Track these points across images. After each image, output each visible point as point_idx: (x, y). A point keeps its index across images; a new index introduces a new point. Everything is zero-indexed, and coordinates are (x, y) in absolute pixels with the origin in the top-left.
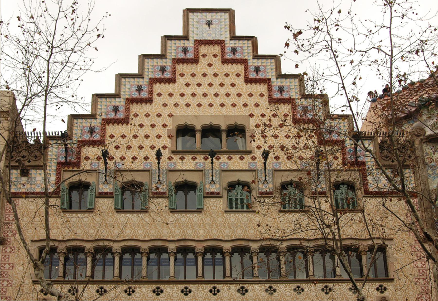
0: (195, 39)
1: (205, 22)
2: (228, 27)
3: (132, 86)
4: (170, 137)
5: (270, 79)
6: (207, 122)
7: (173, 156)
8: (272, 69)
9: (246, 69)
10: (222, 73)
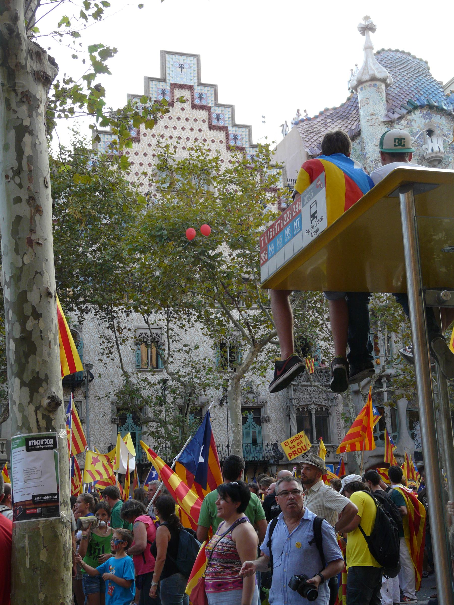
1: (178, 65)
2: (196, 72)
7: (156, 194)
8: (229, 118)
9: (210, 115)
10: (192, 118)
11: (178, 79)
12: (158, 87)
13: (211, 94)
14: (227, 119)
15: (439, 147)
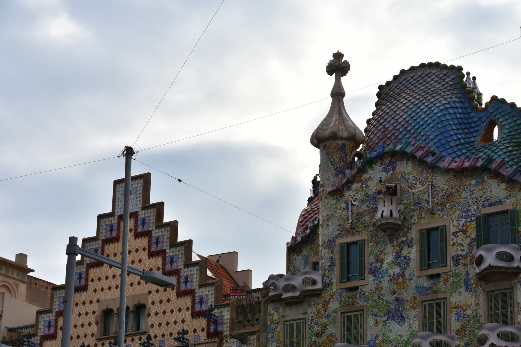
4: (97, 323)
5: (165, 250)
7: (97, 343)
12: (107, 223)
13: (154, 216)
15: (383, 211)
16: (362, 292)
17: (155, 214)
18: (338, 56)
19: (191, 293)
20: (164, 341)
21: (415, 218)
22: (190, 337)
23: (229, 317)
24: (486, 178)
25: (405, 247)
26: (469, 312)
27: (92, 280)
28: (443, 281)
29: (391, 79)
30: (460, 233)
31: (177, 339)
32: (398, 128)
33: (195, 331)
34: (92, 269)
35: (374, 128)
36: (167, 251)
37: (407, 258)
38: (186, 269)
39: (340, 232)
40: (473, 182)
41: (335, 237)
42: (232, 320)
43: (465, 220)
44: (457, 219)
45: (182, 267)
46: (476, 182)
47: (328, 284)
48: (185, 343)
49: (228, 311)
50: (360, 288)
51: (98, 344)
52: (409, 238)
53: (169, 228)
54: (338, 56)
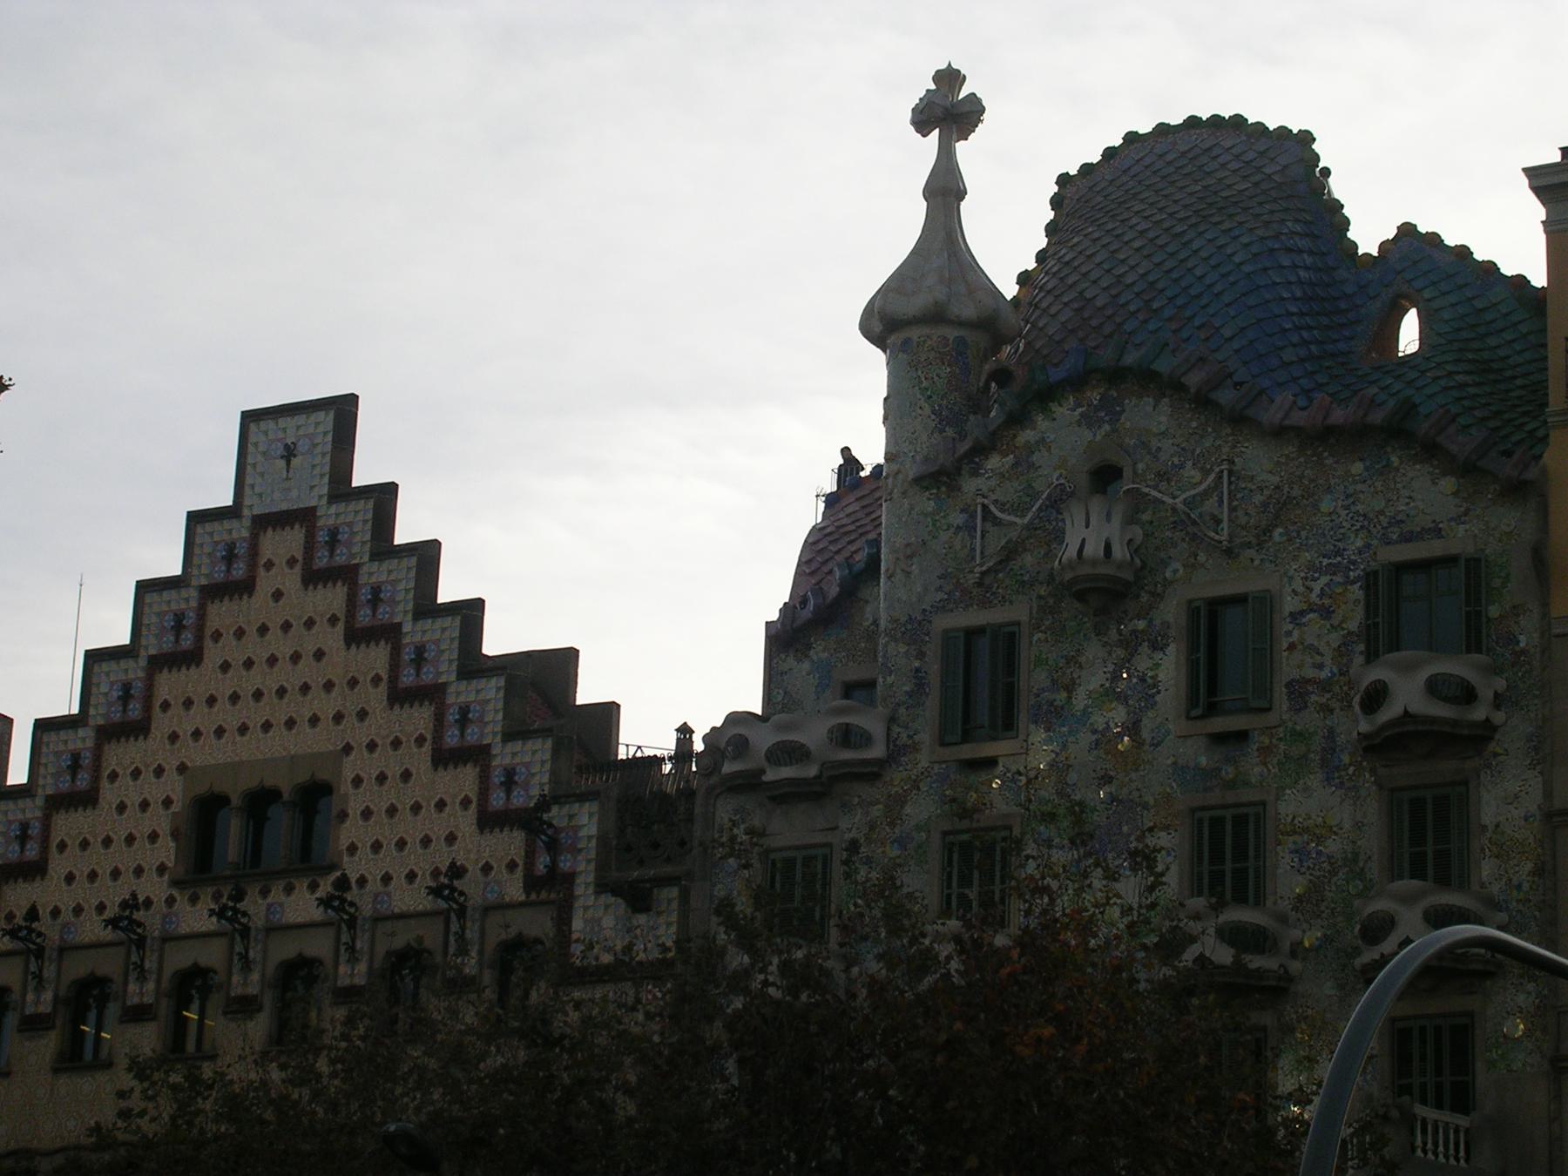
0: (256, 511)
1: (281, 451)
3: (112, 684)
4: (175, 834)
5: (400, 625)
6: (249, 782)
11: (277, 495)
12: (216, 538)
13: (365, 522)
14: (400, 597)
15: (1084, 540)
16: (1008, 775)
17: (370, 516)
18: (949, 78)
19: (478, 755)
20: (388, 894)
21: (1177, 565)
22: (473, 888)
23: (593, 831)
24: (1395, 460)
25: (1145, 648)
26: (1333, 846)
27: (166, 706)
28: (1256, 754)
29: (1095, 158)
30: (1311, 615)
31: (436, 892)
32: (1122, 300)
33: (487, 869)
34: (165, 670)
35: (1050, 299)
36: (407, 628)
37: (1150, 681)
38: (463, 685)
39: (946, 597)
40: (1358, 468)
41: (929, 608)
42: (602, 839)
43: (1329, 577)
44: (1302, 574)
45: (453, 677)
46: (1367, 469)
47: (905, 746)
48: (456, 902)
49: (591, 815)
50: (1001, 761)
51: (178, 899)
52: (1157, 622)
53: (414, 560)
54: (949, 78)
